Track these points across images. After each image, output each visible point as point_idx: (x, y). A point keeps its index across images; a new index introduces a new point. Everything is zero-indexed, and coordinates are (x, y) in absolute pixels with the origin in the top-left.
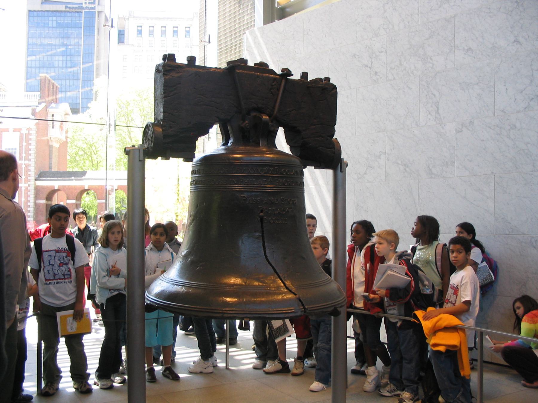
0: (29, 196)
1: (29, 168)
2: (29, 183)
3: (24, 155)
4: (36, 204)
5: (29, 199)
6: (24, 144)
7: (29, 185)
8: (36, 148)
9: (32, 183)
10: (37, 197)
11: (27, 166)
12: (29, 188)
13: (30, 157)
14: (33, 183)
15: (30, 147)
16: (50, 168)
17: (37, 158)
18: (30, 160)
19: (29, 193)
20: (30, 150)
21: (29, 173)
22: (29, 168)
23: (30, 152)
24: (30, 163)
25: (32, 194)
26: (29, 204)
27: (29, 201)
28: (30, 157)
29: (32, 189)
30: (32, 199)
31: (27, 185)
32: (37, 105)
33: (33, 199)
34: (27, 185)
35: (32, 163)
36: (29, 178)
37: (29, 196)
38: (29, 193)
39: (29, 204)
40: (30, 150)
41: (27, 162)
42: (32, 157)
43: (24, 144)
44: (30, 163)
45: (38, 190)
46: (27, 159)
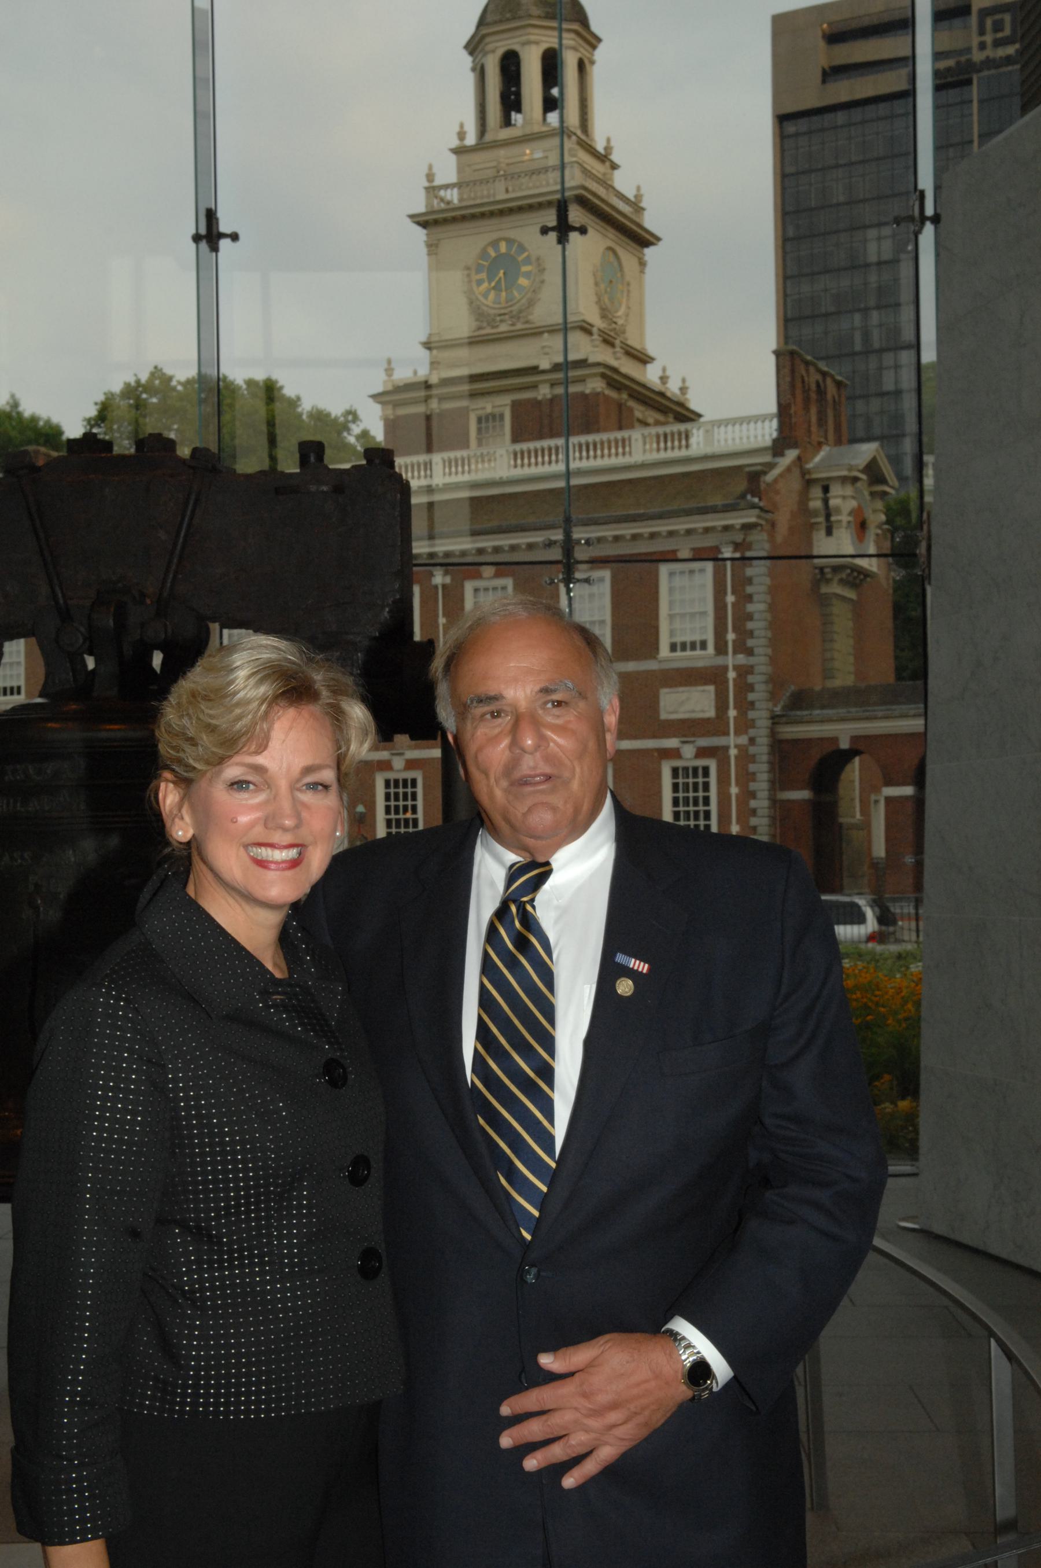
0: (752, 777)
1: (750, 679)
2: (752, 732)
3: (731, 636)
4: (774, 801)
5: (753, 786)
6: (730, 599)
7: (752, 741)
8: (772, 607)
9: (761, 732)
10: (781, 779)
11: (744, 672)
12: (752, 750)
13: (750, 643)
14: (764, 732)
15: (750, 608)
16: (828, 674)
17: (773, 643)
18: (750, 652)
19: (752, 768)
20: (750, 617)
21: (751, 697)
22: (750, 679)
23: (750, 625)
24: (752, 660)
25: (761, 769)
26: (753, 804)
27: (753, 795)
28: (750, 643)
29: (762, 750)
30: (761, 785)
31: (743, 740)
32: (767, 458)
33: (765, 785)
34: (743, 740)
35: (760, 661)
36: (751, 715)
37: (752, 777)
38: (752, 768)
39: (753, 804)
40: (750, 617)
41: (741, 659)
42: (759, 643)
43: (730, 599)
44: (752, 660)
45: (784, 752)
46: (741, 647)
